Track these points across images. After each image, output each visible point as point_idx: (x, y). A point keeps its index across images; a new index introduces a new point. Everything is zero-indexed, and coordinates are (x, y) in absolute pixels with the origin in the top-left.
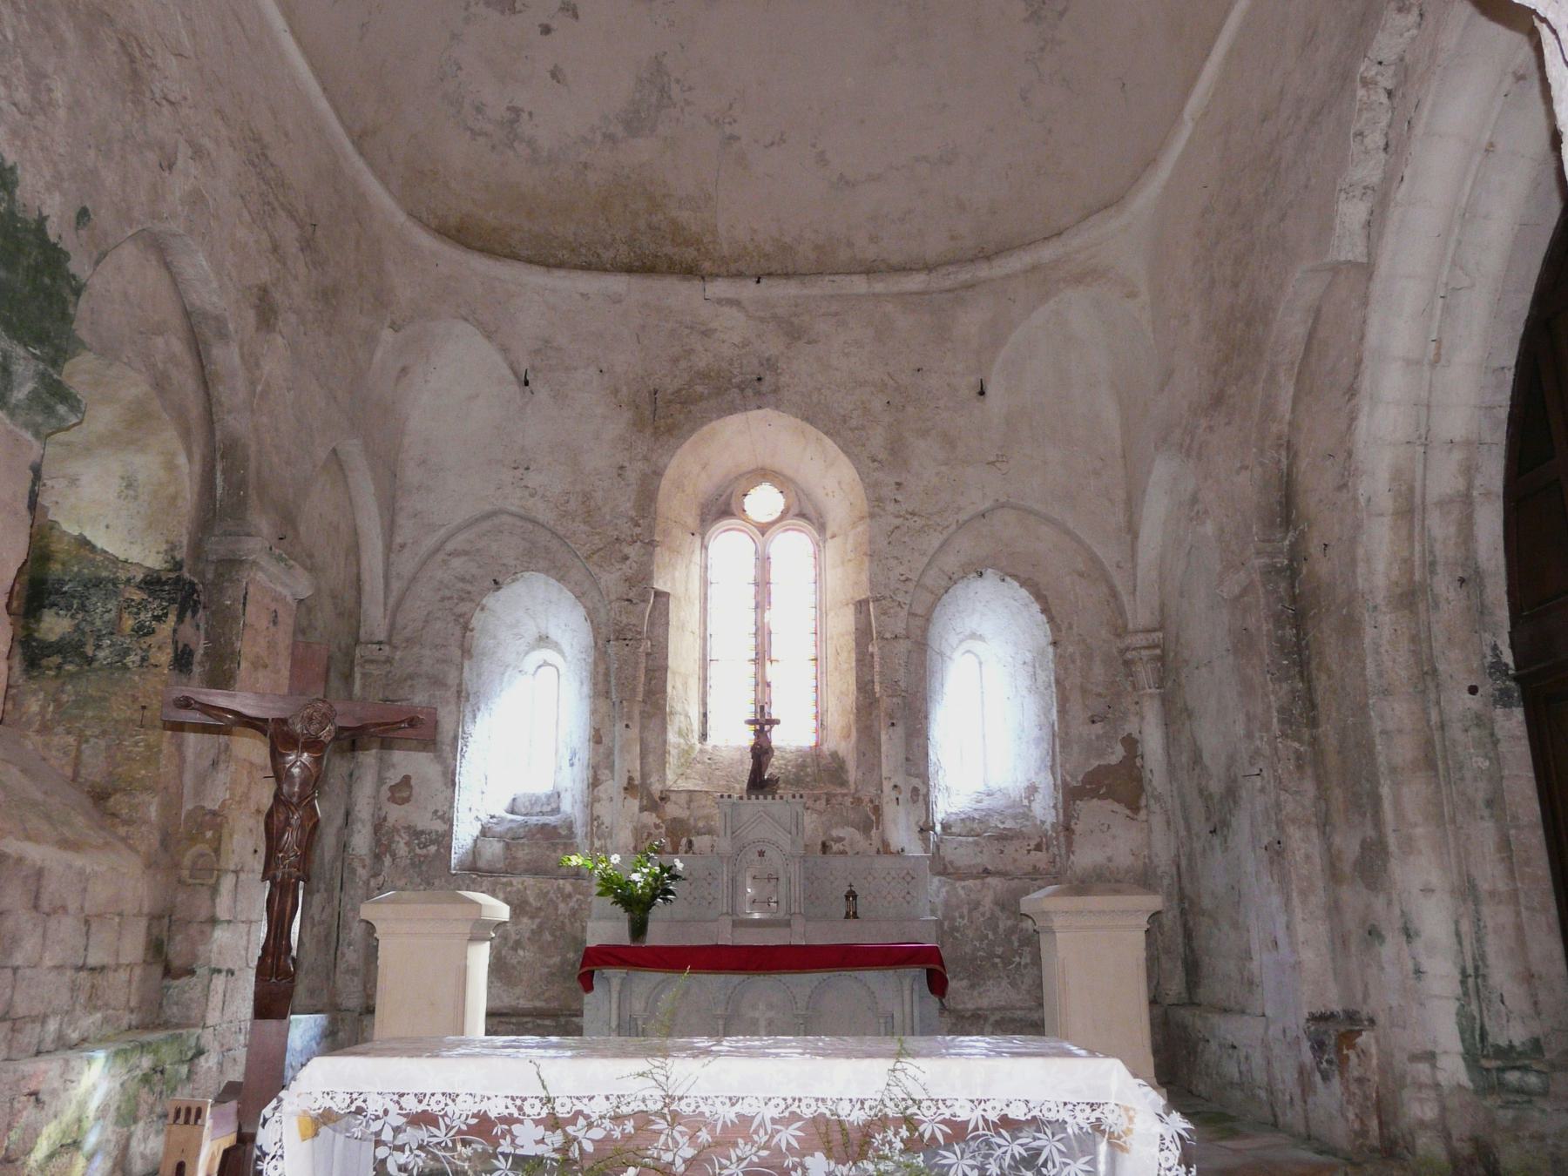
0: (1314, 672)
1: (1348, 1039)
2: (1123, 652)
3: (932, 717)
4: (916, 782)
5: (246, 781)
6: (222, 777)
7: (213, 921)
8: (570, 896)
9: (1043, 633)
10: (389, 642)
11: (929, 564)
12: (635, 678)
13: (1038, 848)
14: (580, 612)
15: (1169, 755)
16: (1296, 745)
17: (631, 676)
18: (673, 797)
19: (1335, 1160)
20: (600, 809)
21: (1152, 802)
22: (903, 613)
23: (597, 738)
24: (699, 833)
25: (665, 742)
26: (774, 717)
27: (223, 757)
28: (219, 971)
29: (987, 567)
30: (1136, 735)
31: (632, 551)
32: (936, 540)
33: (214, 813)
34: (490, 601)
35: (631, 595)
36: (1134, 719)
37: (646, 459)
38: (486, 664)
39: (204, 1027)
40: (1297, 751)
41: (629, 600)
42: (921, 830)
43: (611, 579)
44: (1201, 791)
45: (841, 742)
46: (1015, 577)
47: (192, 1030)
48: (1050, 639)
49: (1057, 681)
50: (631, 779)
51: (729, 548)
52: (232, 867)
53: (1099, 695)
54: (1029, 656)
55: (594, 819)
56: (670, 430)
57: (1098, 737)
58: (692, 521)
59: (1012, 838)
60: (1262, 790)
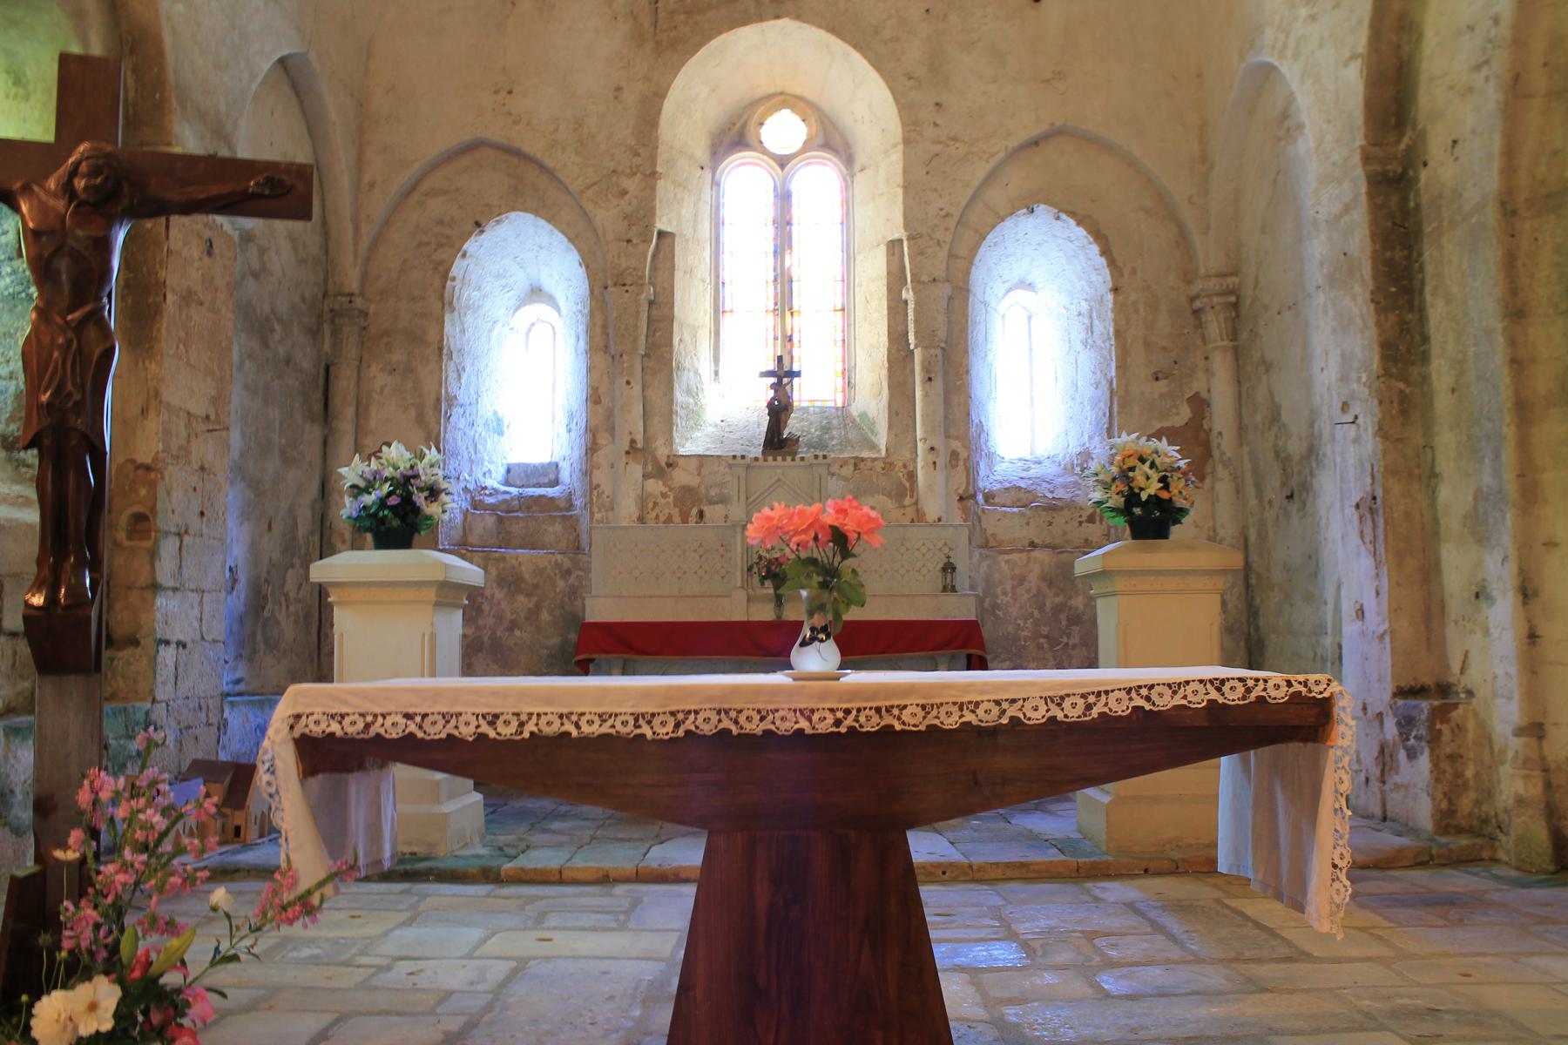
0: (1428, 299)
1: (1441, 714)
2: (1192, 299)
3: (973, 372)
4: (956, 445)
5: (184, 434)
6: (152, 425)
7: (155, 587)
8: (569, 572)
9: (1102, 278)
10: (362, 294)
11: (974, 198)
12: (636, 328)
13: (1091, 519)
14: (574, 257)
15: (1239, 416)
16: (1401, 385)
17: (633, 334)
18: (681, 462)
19: (1479, 841)
20: (600, 477)
21: (1219, 468)
22: (943, 254)
23: (594, 397)
24: (711, 502)
25: (671, 401)
26: (795, 369)
27: (153, 403)
28: (167, 643)
29: (1039, 202)
30: (1204, 395)
31: (632, 185)
32: (981, 170)
33: (148, 468)
34: (471, 246)
35: (630, 235)
36: (1201, 375)
37: (646, 78)
38: (469, 319)
39: (154, 701)
40: (1401, 392)
41: (629, 241)
42: (961, 499)
43: (607, 216)
44: (1277, 453)
45: (872, 400)
46: (1072, 214)
47: (138, 704)
48: (1110, 285)
49: (1118, 333)
50: (633, 441)
51: (744, 185)
52: (173, 530)
53: (1165, 349)
54: (1085, 306)
55: (592, 488)
56: (673, 44)
57: (1162, 396)
58: (701, 151)
59: (1062, 509)
60: (1356, 441)
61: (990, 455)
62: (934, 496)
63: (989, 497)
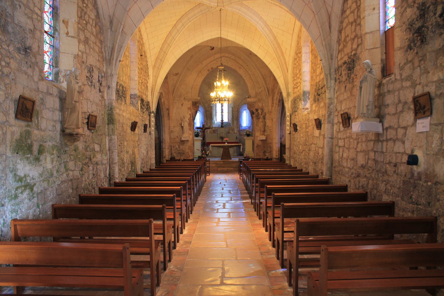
45: (231, 122)
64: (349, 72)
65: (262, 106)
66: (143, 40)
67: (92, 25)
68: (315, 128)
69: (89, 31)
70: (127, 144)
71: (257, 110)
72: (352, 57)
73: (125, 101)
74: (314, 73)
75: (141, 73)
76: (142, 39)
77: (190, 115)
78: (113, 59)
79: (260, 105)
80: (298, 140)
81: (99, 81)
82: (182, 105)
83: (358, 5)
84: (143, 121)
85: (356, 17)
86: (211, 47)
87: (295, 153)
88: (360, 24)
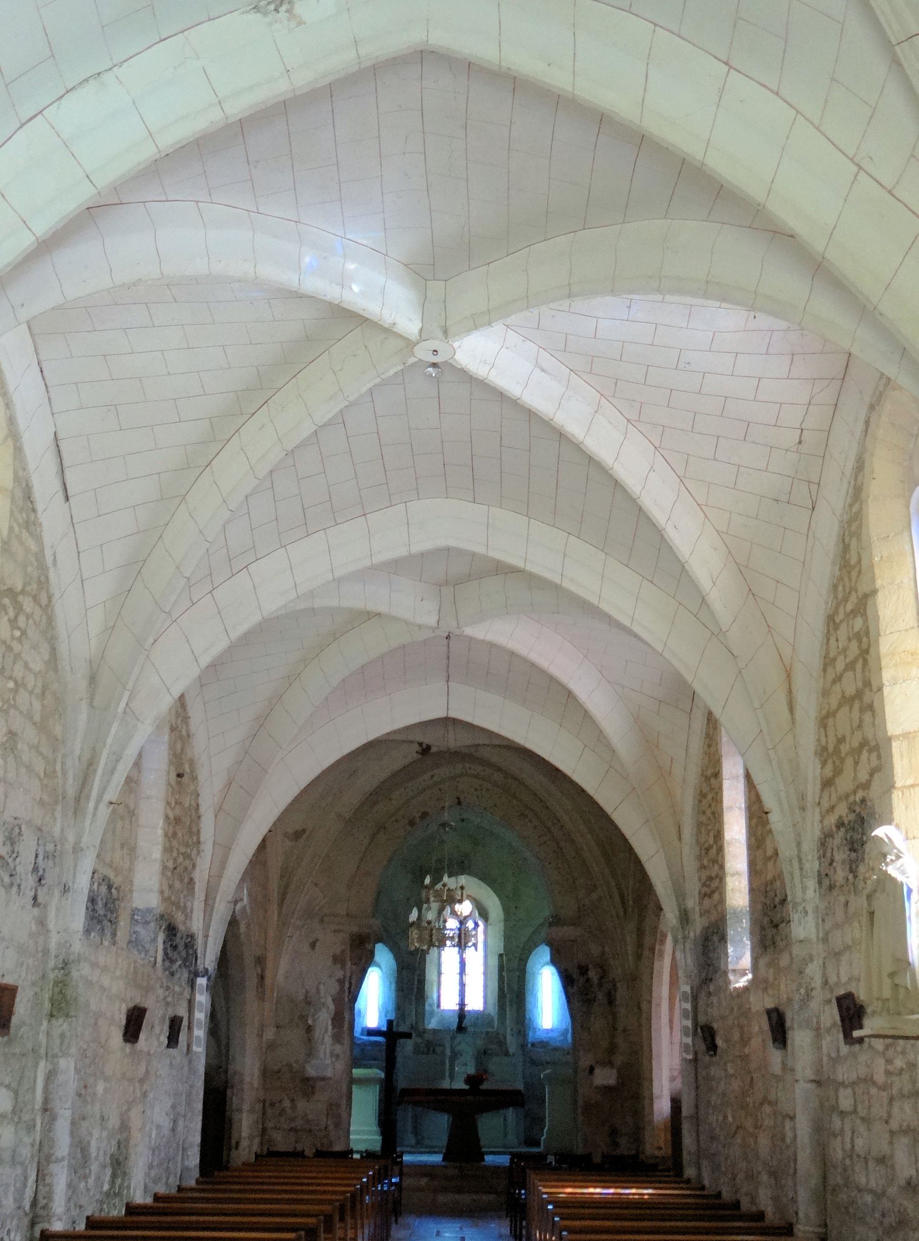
3: (527, 999)
45: (493, 1011)
61: (535, 1029)
62: (512, 1044)
63: (533, 1045)
64: (853, 855)
65: (603, 953)
66: (187, 724)
67: (31, 693)
68: (770, 1042)
69: (21, 713)
70: (105, 1090)
71: (583, 970)
72: (858, 810)
73: (114, 934)
74: (758, 847)
75: (175, 834)
76: (186, 719)
77: (341, 982)
78: (88, 797)
79: (595, 949)
80: (722, 1086)
81: (35, 869)
82: (313, 945)
83: (864, 646)
84: (168, 1004)
85: (860, 685)
86: (420, 744)
87: (713, 1138)
88: (871, 707)
